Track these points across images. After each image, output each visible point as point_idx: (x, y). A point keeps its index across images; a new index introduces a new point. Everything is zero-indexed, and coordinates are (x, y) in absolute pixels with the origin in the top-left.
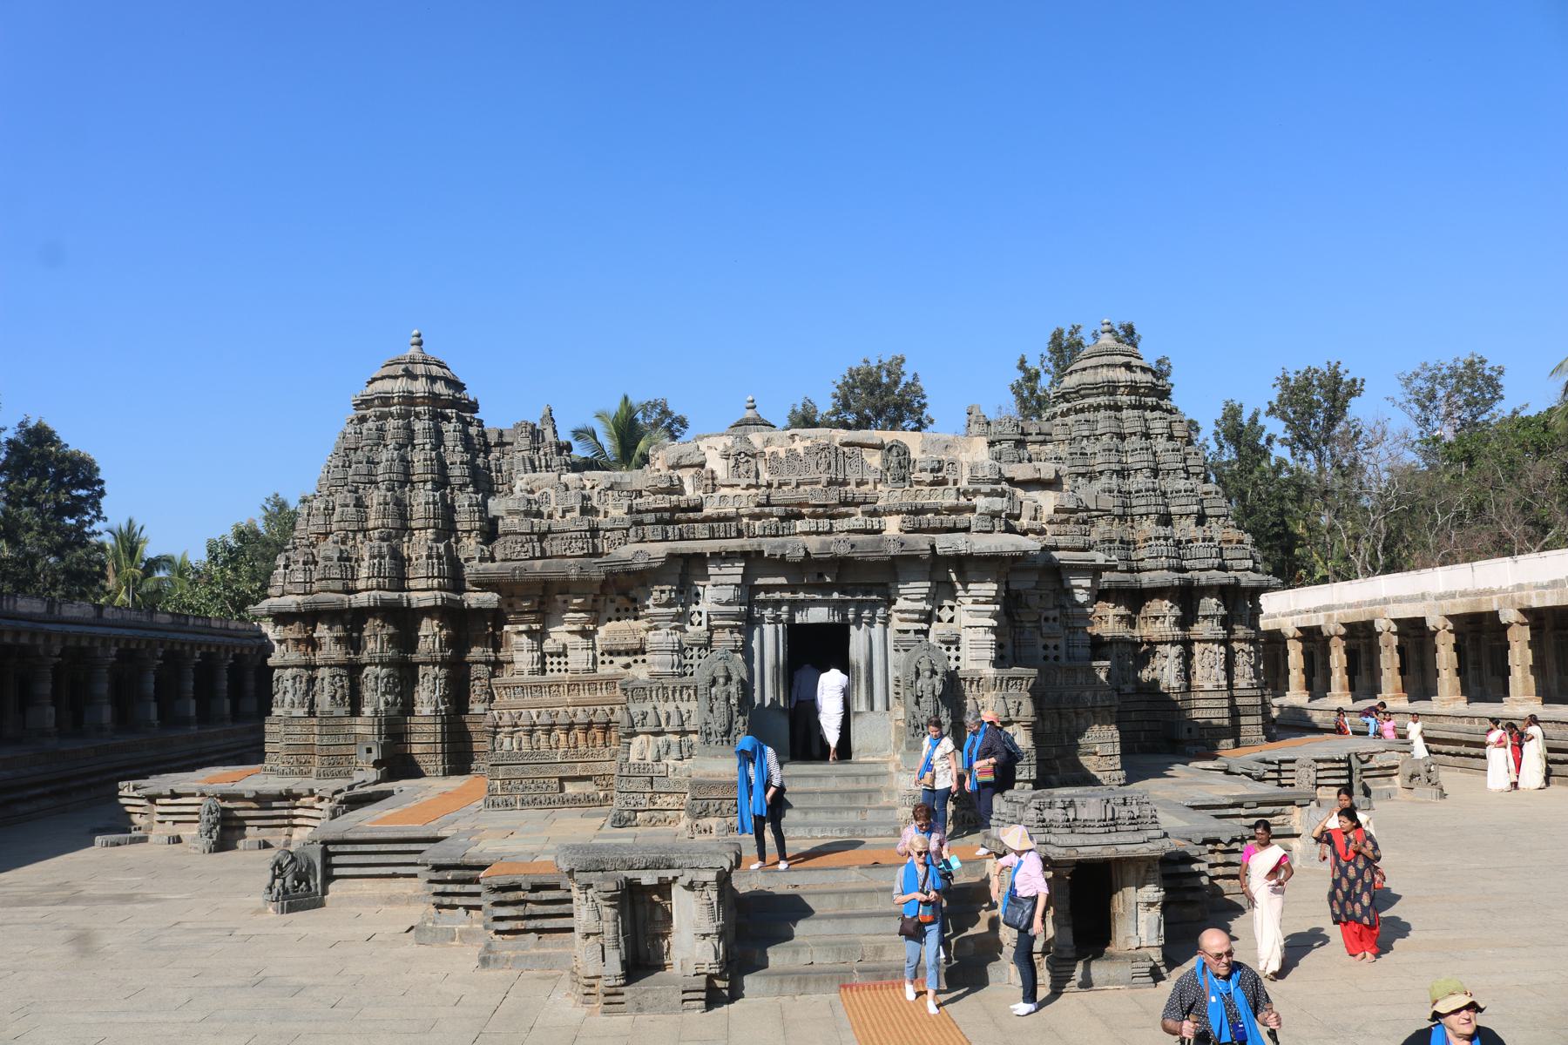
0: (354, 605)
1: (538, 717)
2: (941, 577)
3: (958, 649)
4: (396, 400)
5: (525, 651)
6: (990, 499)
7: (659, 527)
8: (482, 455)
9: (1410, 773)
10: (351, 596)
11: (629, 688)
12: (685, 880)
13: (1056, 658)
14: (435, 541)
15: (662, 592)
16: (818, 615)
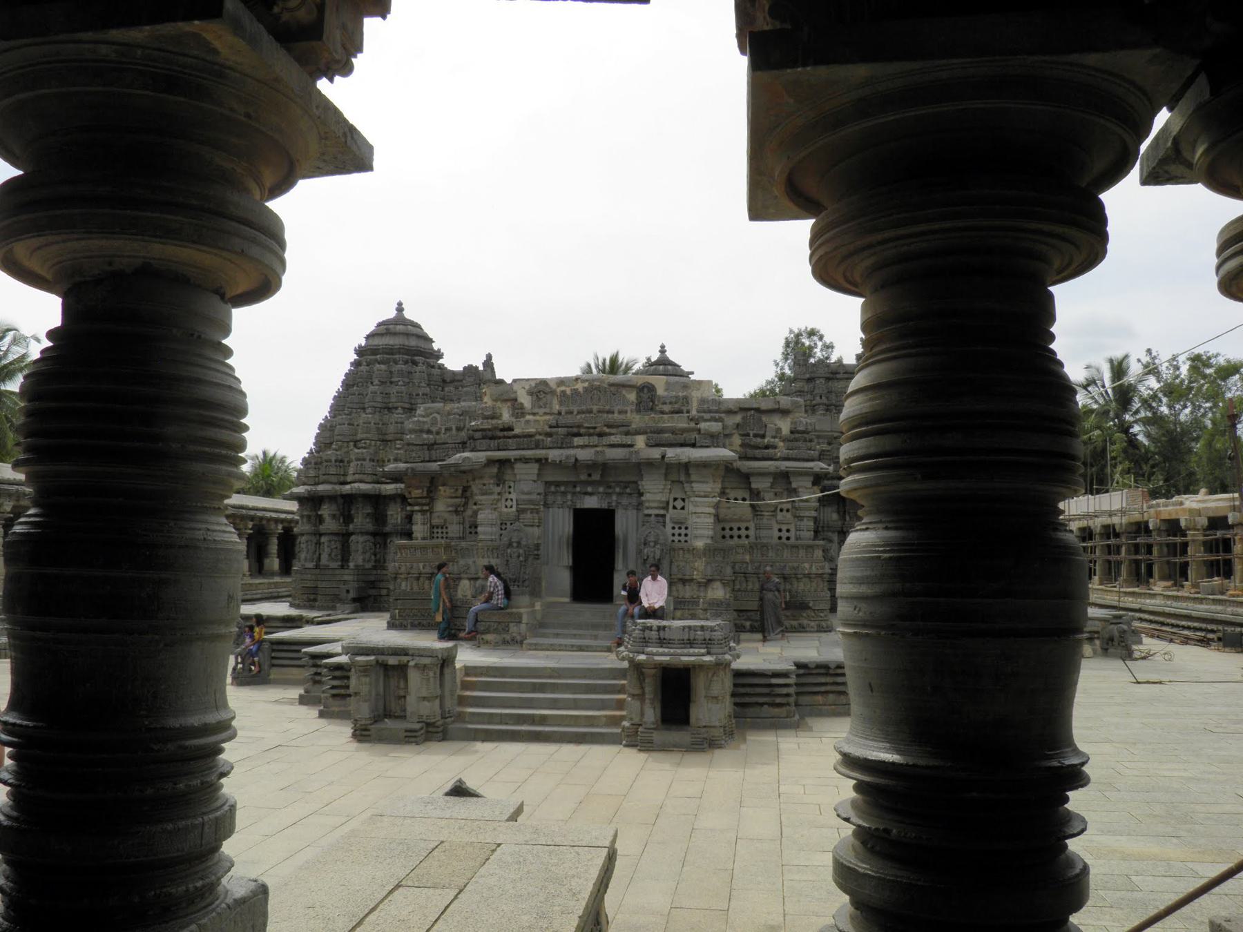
0: (344, 493)
1: (424, 568)
2: (675, 477)
3: (686, 528)
4: (381, 351)
5: (419, 522)
6: (708, 424)
7: (484, 441)
8: (440, 388)
9: (1107, 636)
10: (341, 487)
11: (459, 548)
12: (412, 663)
13: (788, 538)
14: (399, 449)
15: (484, 485)
16: (591, 502)
